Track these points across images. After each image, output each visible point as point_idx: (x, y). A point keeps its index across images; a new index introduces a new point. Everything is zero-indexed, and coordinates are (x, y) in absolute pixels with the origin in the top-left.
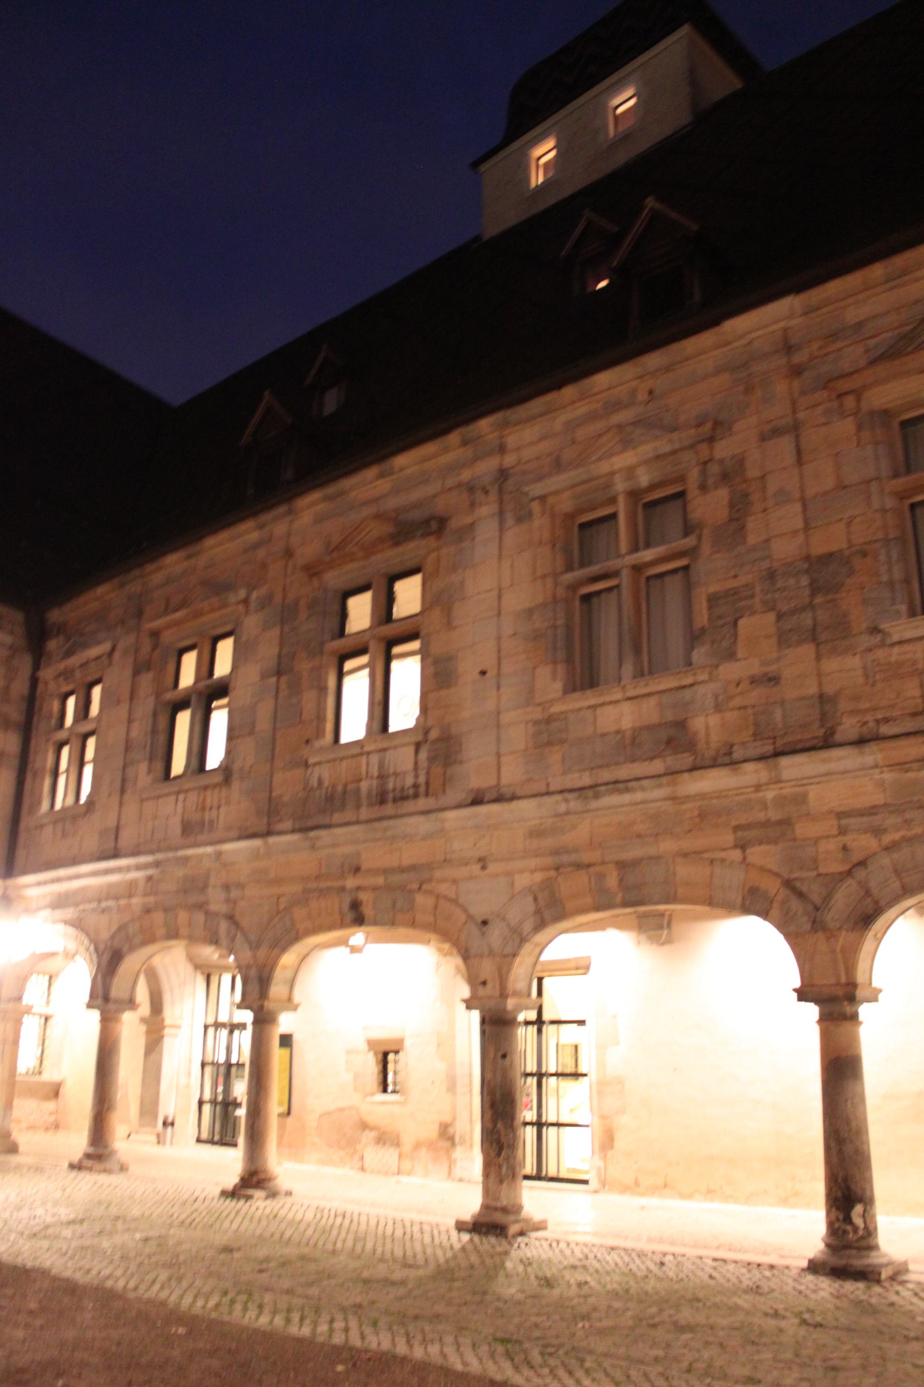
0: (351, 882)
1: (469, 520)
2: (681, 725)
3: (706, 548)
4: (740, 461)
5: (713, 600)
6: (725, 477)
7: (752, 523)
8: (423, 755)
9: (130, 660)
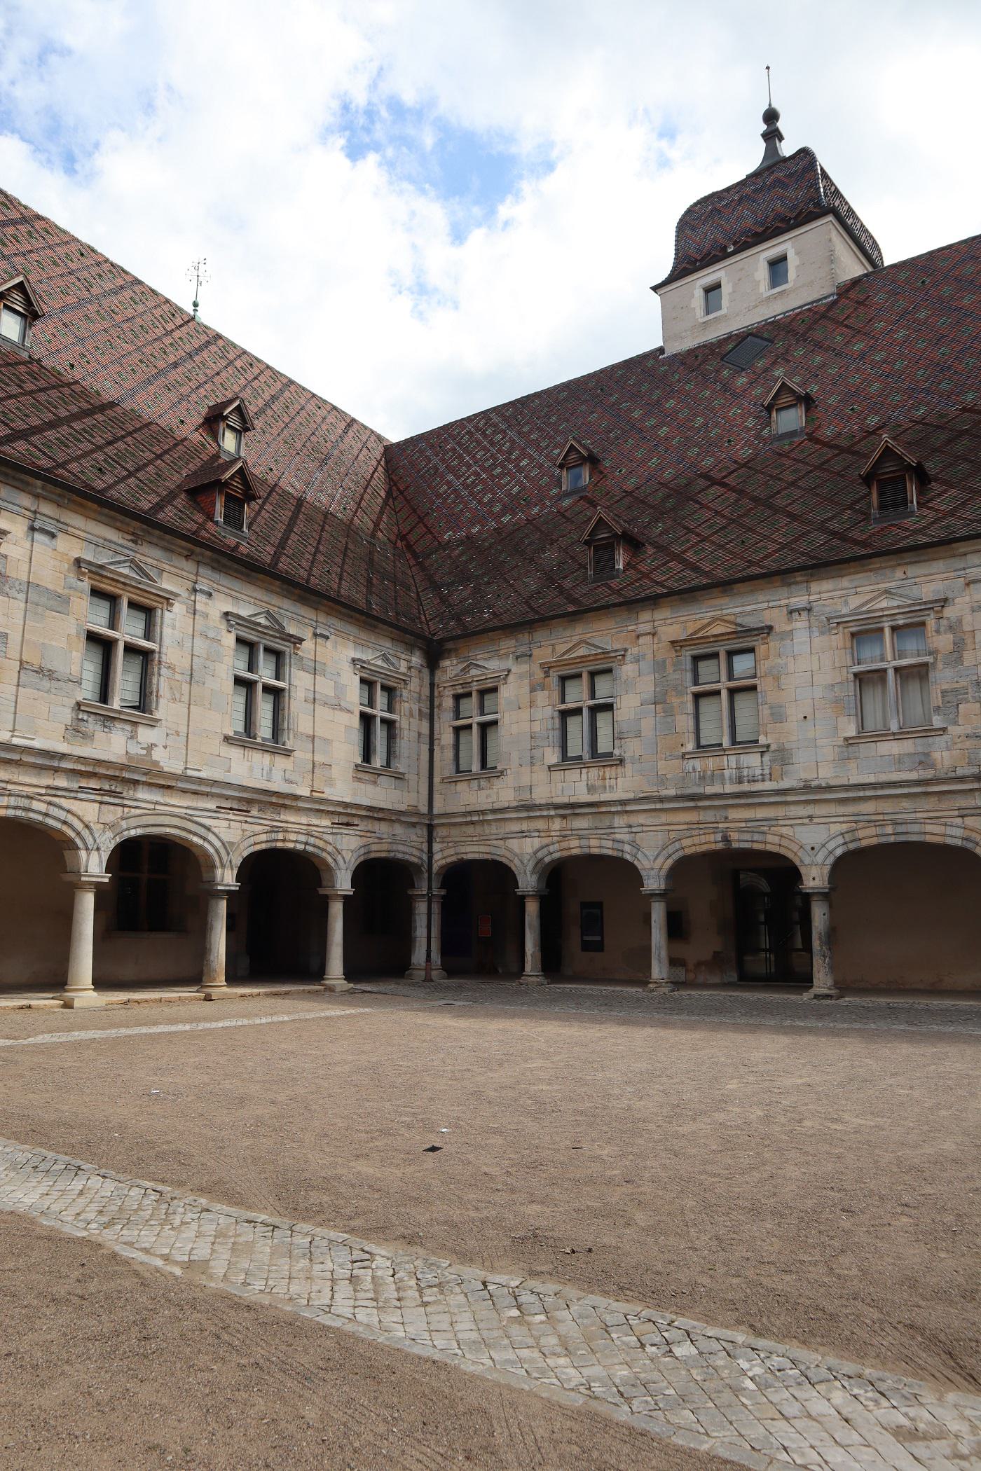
0: (721, 826)
1: (788, 628)
2: (927, 755)
3: (940, 665)
4: (960, 621)
5: (944, 693)
6: (951, 628)
7: (966, 655)
8: (767, 758)
9: (527, 682)
